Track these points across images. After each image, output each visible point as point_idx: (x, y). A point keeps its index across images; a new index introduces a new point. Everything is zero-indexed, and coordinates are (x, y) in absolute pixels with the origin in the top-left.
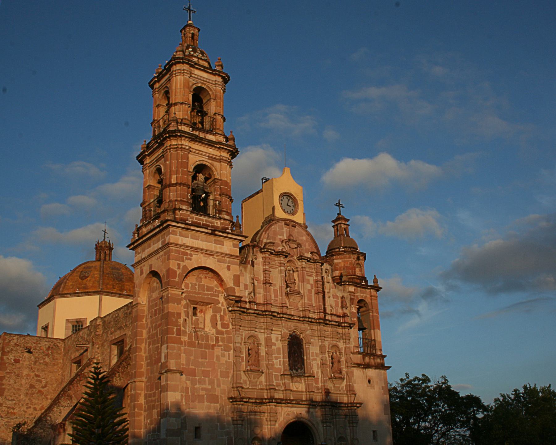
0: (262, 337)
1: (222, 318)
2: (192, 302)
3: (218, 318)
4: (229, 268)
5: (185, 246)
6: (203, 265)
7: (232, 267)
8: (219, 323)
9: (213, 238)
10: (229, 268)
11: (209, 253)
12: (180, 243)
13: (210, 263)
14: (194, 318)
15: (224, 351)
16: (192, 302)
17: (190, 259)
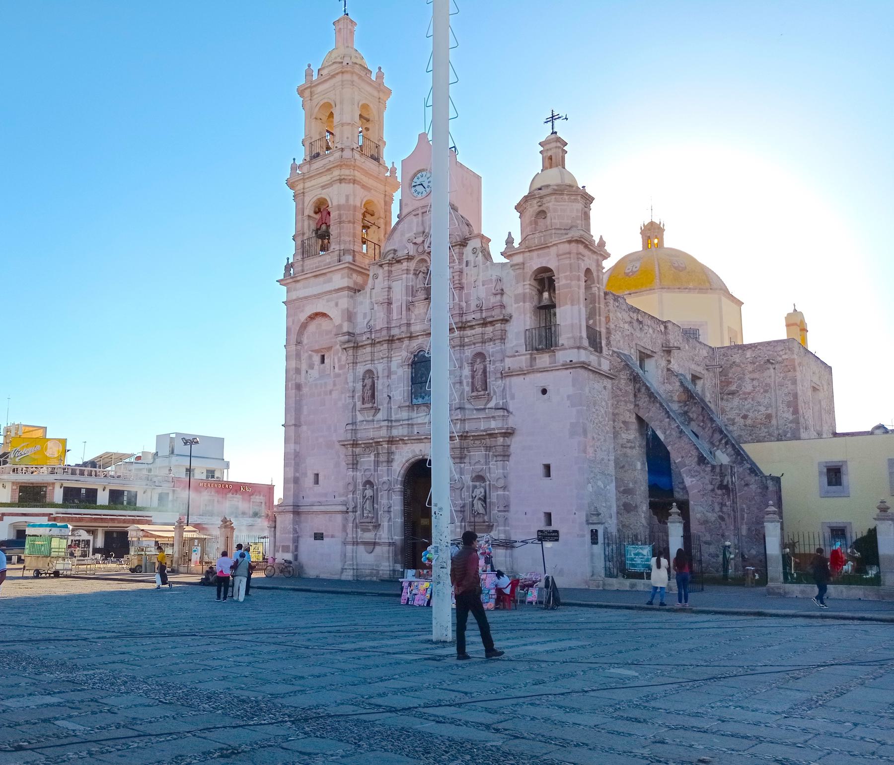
0: (380, 367)
1: (339, 360)
2: (316, 351)
3: (336, 361)
4: (337, 305)
5: (298, 299)
6: (315, 311)
7: (340, 301)
8: (336, 366)
9: (321, 279)
10: (337, 305)
11: (318, 296)
12: (294, 298)
13: (320, 307)
14: (322, 366)
15: (342, 393)
16: (316, 351)
17: (302, 311)
